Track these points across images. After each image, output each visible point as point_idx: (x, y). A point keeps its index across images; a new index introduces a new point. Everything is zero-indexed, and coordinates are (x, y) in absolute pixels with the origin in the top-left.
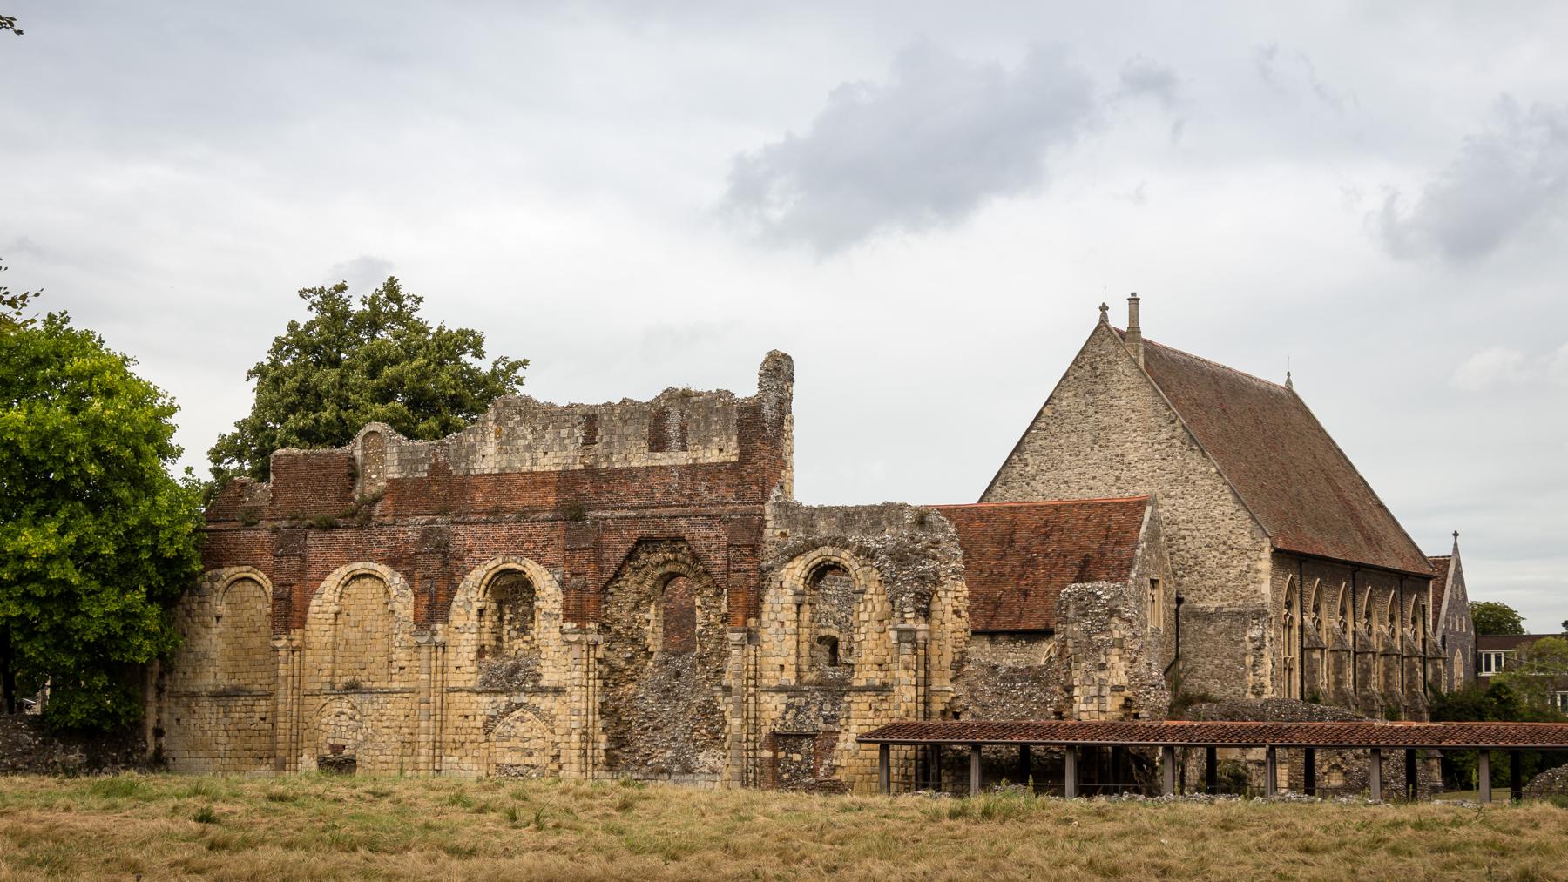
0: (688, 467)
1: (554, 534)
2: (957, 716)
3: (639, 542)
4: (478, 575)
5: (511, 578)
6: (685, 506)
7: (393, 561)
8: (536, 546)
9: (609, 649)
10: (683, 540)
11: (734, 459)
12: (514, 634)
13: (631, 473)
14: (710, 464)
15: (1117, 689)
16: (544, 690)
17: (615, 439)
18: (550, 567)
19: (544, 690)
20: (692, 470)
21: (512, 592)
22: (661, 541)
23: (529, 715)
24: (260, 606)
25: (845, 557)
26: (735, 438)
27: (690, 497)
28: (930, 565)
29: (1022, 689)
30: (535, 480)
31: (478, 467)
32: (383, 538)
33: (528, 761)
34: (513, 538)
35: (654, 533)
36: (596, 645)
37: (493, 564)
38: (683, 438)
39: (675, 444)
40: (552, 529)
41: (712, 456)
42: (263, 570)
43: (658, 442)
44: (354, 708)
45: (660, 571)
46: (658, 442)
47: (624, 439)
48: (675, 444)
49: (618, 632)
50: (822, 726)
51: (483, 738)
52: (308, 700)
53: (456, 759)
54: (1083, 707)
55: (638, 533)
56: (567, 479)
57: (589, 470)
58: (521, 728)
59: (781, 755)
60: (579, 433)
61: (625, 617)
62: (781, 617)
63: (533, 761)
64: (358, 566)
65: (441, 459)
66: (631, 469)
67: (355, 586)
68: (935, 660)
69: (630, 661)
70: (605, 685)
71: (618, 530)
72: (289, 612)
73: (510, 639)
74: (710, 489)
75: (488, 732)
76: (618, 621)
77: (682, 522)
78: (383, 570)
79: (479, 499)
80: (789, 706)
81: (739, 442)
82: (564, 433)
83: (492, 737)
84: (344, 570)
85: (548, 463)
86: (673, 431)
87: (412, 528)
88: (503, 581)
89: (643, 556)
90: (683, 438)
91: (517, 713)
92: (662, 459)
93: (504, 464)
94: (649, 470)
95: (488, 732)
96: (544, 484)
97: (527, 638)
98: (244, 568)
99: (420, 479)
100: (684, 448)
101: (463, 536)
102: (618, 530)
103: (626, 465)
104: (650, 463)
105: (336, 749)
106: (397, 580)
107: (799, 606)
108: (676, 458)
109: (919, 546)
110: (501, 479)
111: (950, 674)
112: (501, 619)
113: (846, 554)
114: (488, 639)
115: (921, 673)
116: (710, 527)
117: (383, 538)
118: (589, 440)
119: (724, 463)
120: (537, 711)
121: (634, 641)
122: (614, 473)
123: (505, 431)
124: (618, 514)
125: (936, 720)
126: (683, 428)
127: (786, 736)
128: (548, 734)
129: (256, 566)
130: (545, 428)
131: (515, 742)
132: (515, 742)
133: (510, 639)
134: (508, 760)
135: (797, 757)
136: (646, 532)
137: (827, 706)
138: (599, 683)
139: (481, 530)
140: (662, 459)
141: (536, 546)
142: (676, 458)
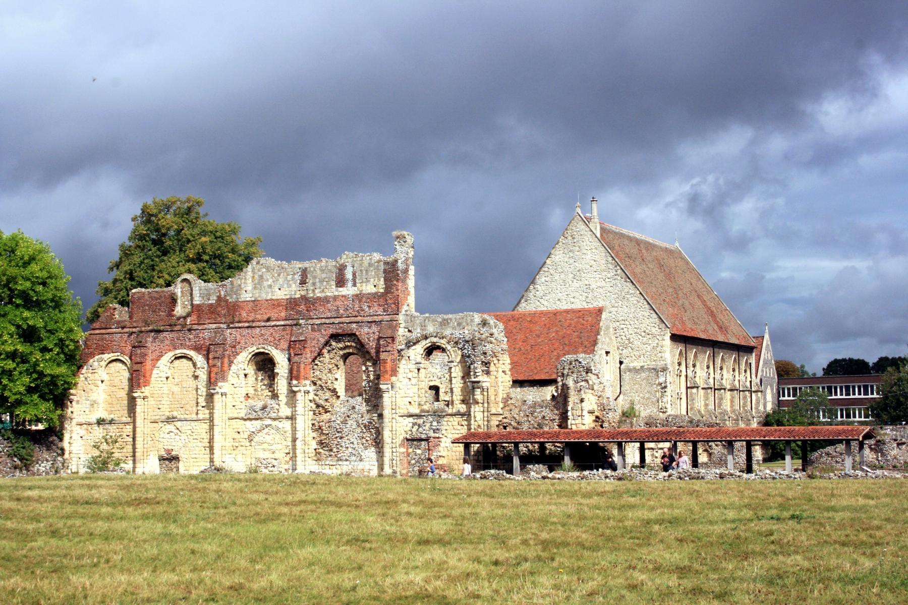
0: (357, 295)
2: (505, 428)
6: (356, 316)
7: (197, 349)
8: (275, 339)
9: (316, 395)
10: (355, 335)
11: (382, 291)
13: (326, 300)
14: (369, 294)
15: (591, 412)
17: (317, 280)
20: (359, 297)
22: (342, 335)
23: (273, 431)
25: (443, 343)
26: (382, 279)
27: (358, 311)
28: (489, 347)
29: (539, 413)
30: (275, 304)
32: (191, 337)
33: (273, 456)
34: (262, 335)
35: (340, 331)
36: (308, 392)
38: (354, 280)
39: (350, 284)
40: (284, 330)
41: (369, 289)
45: (341, 353)
47: (321, 281)
48: (350, 284)
50: (432, 434)
51: (248, 444)
54: (573, 422)
55: (331, 331)
56: (292, 303)
57: (304, 298)
58: (268, 439)
59: (410, 450)
60: (298, 277)
62: (410, 375)
63: (276, 456)
64: (179, 352)
65: (222, 293)
67: (177, 362)
68: (492, 398)
71: (320, 330)
73: (262, 390)
74: (369, 307)
75: (251, 441)
76: (320, 379)
77: (354, 325)
78: (192, 353)
79: (244, 314)
80: (414, 424)
81: (385, 280)
82: (290, 277)
83: (253, 443)
84: (170, 354)
85: (281, 294)
86: (349, 275)
87: (208, 331)
89: (334, 343)
90: (354, 280)
91: (266, 430)
92: (343, 291)
94: (335, 298)
95: (251, 441)
96: (279, 305)
99: (211, 304)
102: (320, 330)
104: (336, 293)
105: (168, 451)
106: (200, 359)
107: (419, 370)
108: (349, 290)
109: (484, 336)
111: (501, 405)
112: (256, 379)
113: (442, 341)
115: (486, 405)
116: (370, 328)
118: (303, 282)
119: (376, 293)
120: (278, 429)
122: (319, 298)
123: (256, 276)
124: (318, 322)
125: (494, 429)
126: (354, 274)
127: (413, 440)
128: (283, 442)
129: (122, 353)
130: (279, 275)
131: (265, 446)
132: (265, 446)
133: (262, 390)
135: (419, 451)
136: (335, 331)
137: (435, 424)
140: (343, 291)
141: (275, 339)
142: (349, 290)
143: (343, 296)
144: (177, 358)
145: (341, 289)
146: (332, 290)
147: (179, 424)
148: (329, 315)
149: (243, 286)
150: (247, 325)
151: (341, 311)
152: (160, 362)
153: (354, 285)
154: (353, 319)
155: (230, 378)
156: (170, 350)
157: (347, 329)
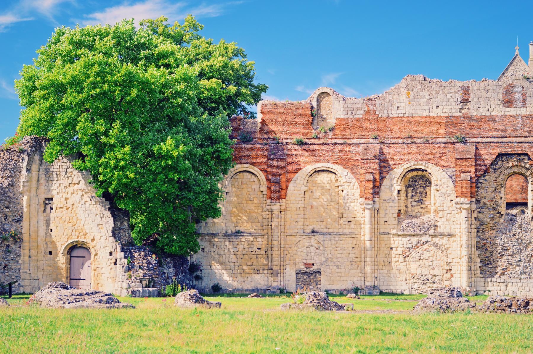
1: (446, 150)
3: (500, 155)
4: (399, 171)
5: (415, 173)
6: (526, 137)
9: (480, 212)
12: (414, 203)
13: (493, 119)
16: (442, 235)
18: (444, 168)
19: (442, 235)
21: (418, 181)
23: (433, 248)
24: (254, 187)
30: (430, 121)
31: (395, 113)
33: (432, 272)
35: (509, 151)
37: (409, 165)
42: (258, 167)
43: (508, 102)
44: (319, 243)
46: (508, 102)
49: (485, 204)
52: (289, 238)
53: (386, 271)
56: (451, 122)
58: (426, 255)
60: (459, 96)
61: (490, 195)
64: (319, 166)
65: (371, 108)
66: (492, 117)
69: (492, 219)
70: (478, 232)
72: (277, 190)
79: (396, 130)
86: (517, 96)
88: (410, 175)
91: (425, 246)
93: (411, 112)
94: (504, 117)
97: (422, 206)
98: (245, 165)
99: (359, 119)
100: (524, 106)
101: (388, 152)
103: (488, 114)
105: (307, 265)
110: (409, 120)
114: (403, 208)
117: (336, 151)
118: (465, 101)
120: (437, 246)
121: (494, 209)
123: (412, 94)
126: (524, 96)
129: (253, 164)
134: (419, 271)
138: (476, 230)
139: (399, 147)
140: (510, 111)
143: (511, 116)
144: (317, 172)
145: (508, 109)
146: (498, 110)
147: (321, 238)
148: (495, 134)
149: (395, 101)
150: (400, 141)
151: (509, 131)
152: (297, 175)
153: (524, 106)
154: (523, 139)
155: (382, 194)
156: (310, 163)
157: (518, 149)
